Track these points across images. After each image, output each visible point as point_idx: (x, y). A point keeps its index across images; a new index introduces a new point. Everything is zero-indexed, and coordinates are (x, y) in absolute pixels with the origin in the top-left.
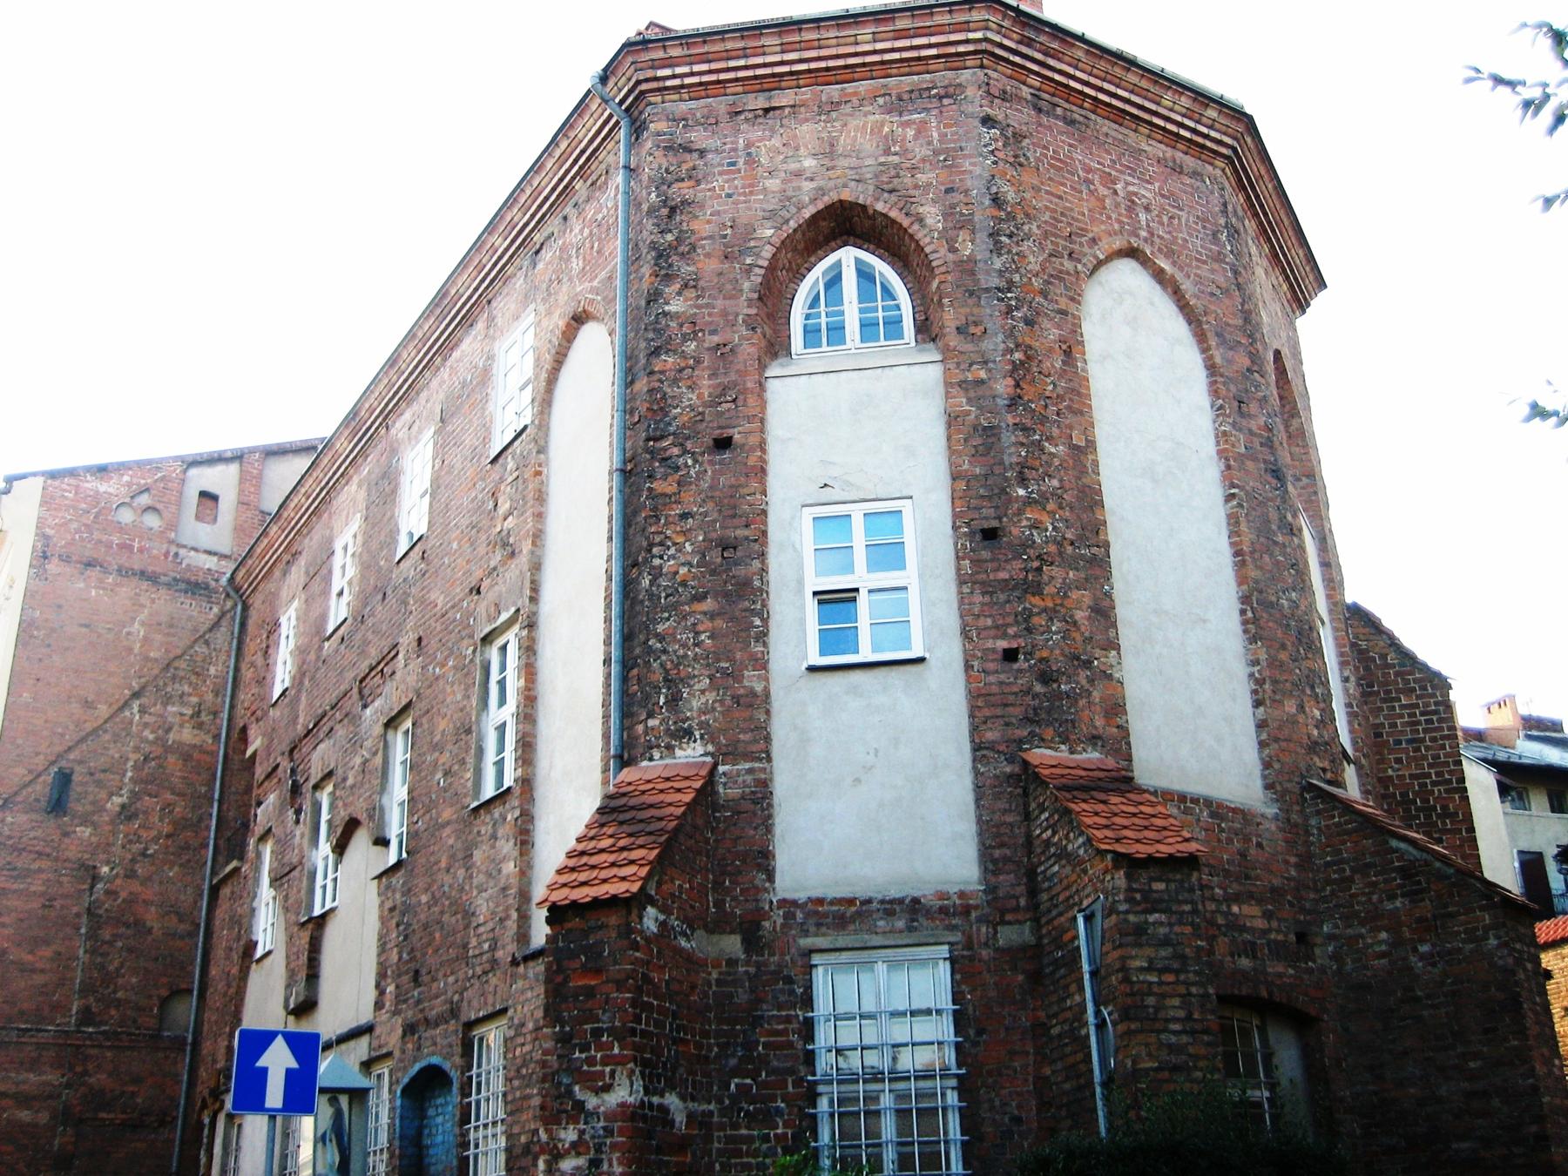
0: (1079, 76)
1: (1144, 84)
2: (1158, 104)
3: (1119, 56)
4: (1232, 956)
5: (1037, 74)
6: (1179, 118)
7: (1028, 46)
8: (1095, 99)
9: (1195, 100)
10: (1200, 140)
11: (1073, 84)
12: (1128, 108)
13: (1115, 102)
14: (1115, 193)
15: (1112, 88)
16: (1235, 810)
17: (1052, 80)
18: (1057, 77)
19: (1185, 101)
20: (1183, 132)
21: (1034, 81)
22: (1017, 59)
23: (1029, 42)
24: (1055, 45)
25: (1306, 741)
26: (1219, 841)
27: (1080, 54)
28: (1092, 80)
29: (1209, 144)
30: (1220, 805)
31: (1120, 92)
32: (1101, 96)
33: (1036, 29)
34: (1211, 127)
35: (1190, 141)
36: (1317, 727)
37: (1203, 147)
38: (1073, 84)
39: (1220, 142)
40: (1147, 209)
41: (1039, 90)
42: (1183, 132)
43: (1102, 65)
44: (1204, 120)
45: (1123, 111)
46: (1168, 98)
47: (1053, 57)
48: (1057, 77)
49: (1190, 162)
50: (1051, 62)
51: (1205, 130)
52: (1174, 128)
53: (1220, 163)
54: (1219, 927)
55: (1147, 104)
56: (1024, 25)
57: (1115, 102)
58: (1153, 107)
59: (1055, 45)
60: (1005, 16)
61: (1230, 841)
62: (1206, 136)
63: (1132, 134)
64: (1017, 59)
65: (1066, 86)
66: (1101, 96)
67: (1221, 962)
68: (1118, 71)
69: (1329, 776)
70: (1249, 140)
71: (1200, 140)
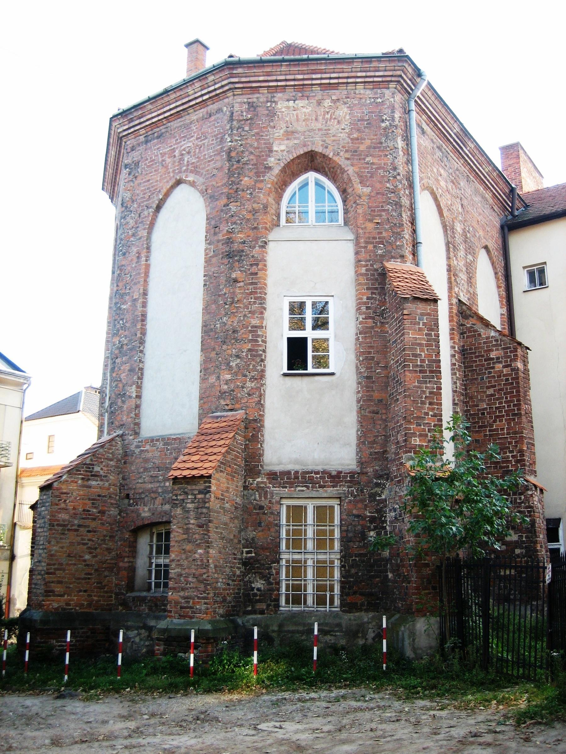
0: (153, 115)
1: (178, 94)
2: (189, 96)
3: (166, 92)
4: (162, 505)
5: (141, 128)
6: (199, 94)
7: (132, 121)
8: (165, 118)
9: (200, 80)
10: (214, 94)
11: (154, 120)
12: (179, 109)
13: (172, 112)
14: (175, 156)
15: (168, 108)
16: (175, 439)
17: (147, 126)
18: (148, 123)
19: (197, 85)
20: (205, 97)
21: (142, 131)
22: (132, 130)
23: (131, 120)
24: (140, 112)
25: (218, 393)
26: (166, 455)
27: (150, 107)
28: (159, 112)
29: (218, 92)
30: (168, 439)
31: (172, 106)
32: (166, 115)
33: (130, 113)
34: (215, 84)
35: (210, 98)
36: (226, 384)
37: (217, 95)
38: (154, 120)
39: (222, 86)
40: (189, 153)
41: (147, 132)
42: (205, 97)
43: (159, 103)
44: (210, 84)
45: (178, 112)
46: (190, 90)
47: (142, 117)
48: (148, 123)
49: (215, 106)
50: (142, 120)
51: (212, 88)
52: (200, 100)
53: (230, 94)
54: (159, 493)
55: (184, 101)
56: (126, 116)
57: (172, 112)
58: (187, 99)
59: (140, 112)
60: (119, 119)
61: (171, 453)
62: (215, 90)
63: (187, 117)
64: (132, 130)
65: (153, 123)
66: (166, 115)
67: (156, 508)
68: (166, 99)
69: (230, 407)
70: (240, 70)
71: (214, 94)
